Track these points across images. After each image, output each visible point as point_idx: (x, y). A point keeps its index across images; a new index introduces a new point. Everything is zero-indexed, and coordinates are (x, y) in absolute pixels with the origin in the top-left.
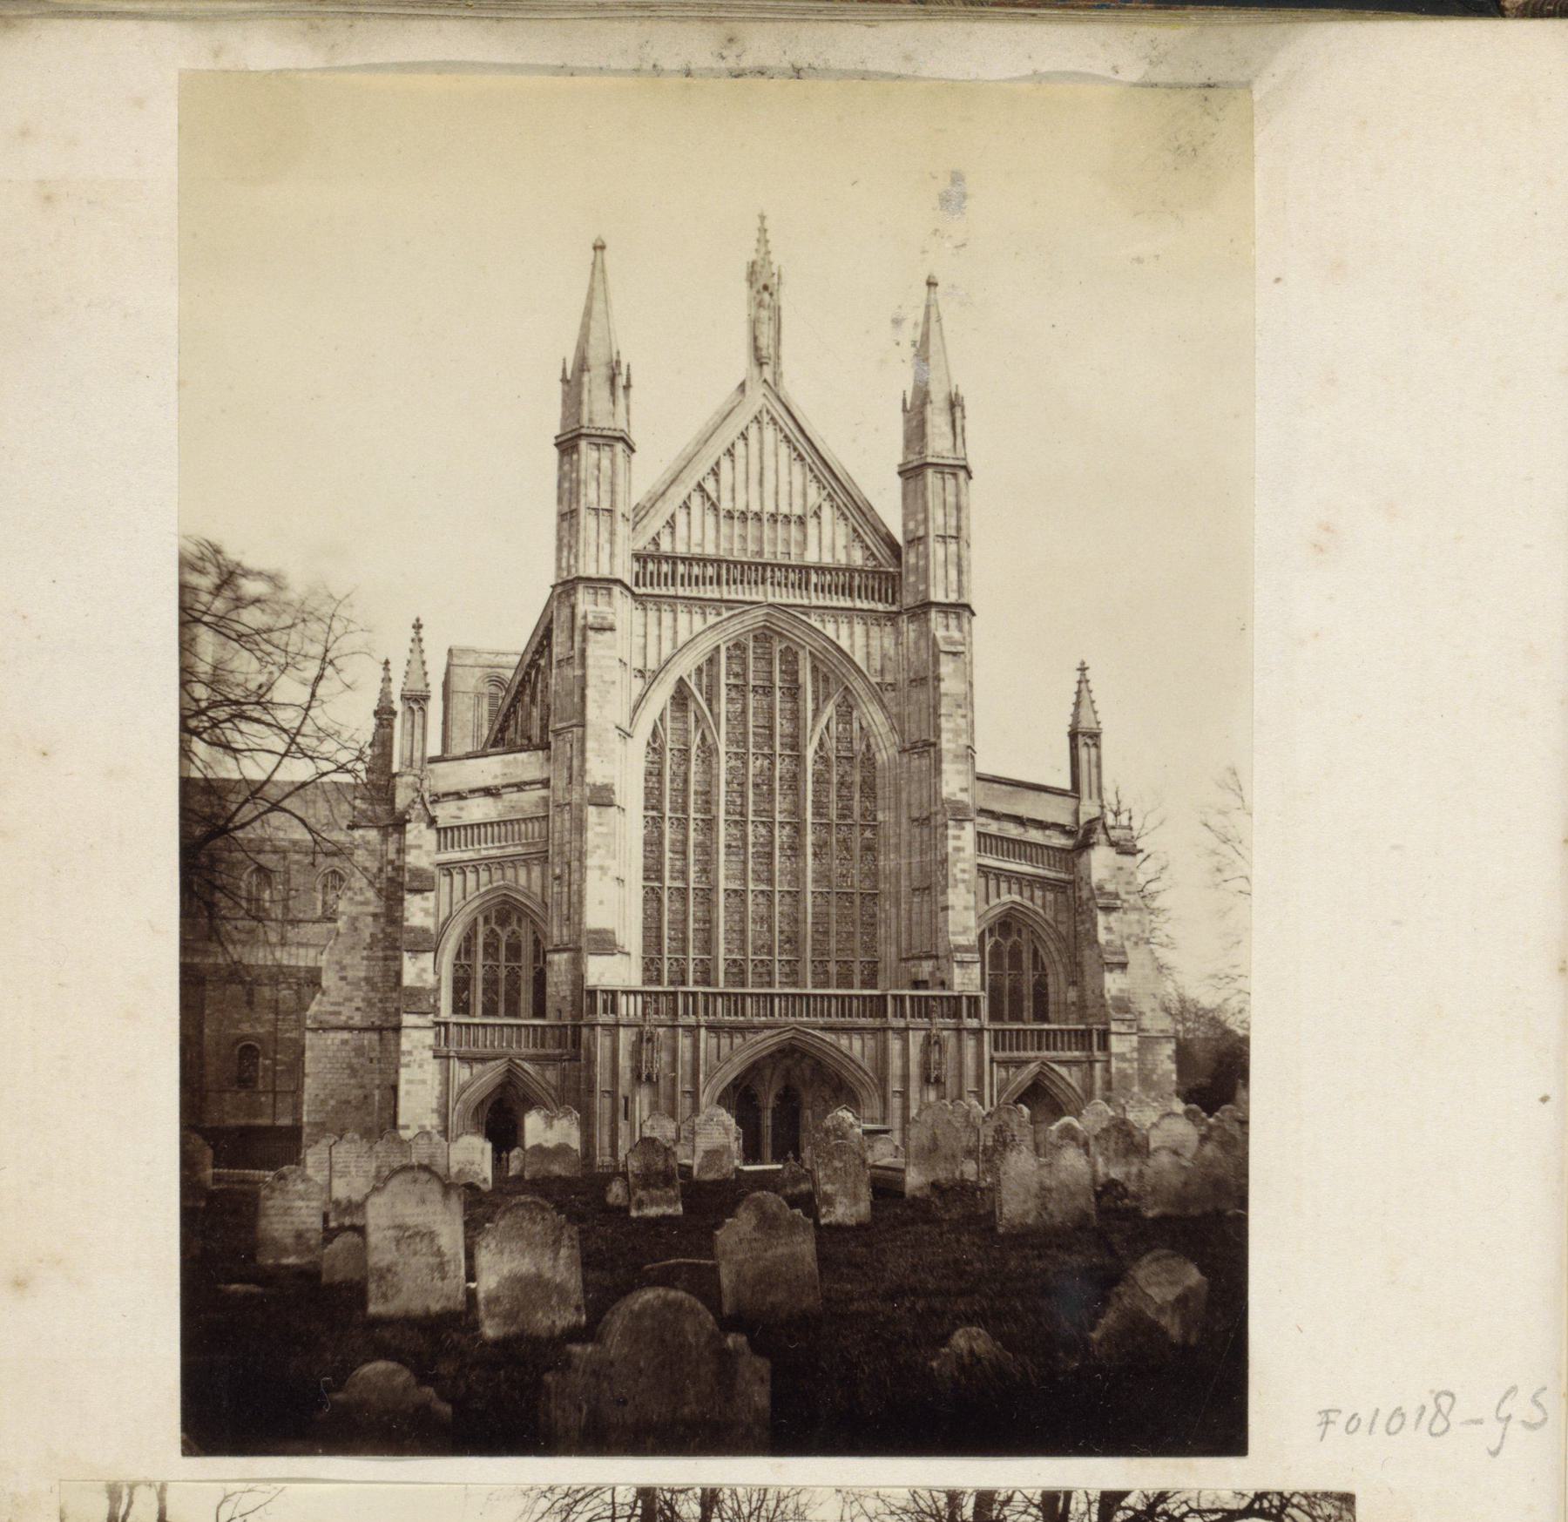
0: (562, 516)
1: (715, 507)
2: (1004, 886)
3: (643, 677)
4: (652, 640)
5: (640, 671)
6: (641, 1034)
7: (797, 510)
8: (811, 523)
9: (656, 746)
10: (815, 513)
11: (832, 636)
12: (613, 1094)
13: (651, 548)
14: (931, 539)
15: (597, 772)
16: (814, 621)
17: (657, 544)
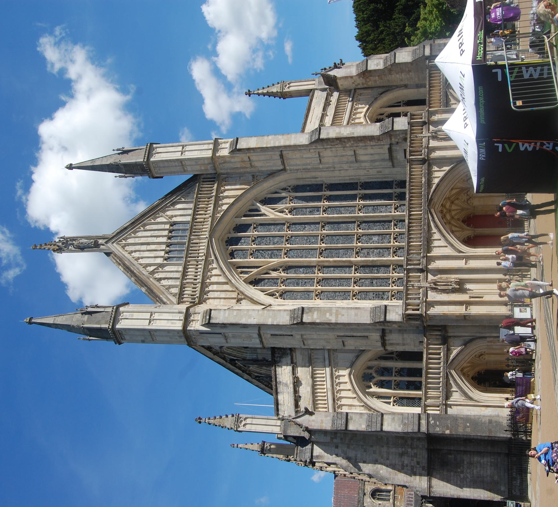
0: (153, 341)
1: (161, 266)
2: (357, 121)
3: (241, 299)
4: (223, 295)
5: (237, 301)
6: (432, 289)
7: (167, 226)
8: (175, 219)
9: (277, 294)
10: (169, 218)
11: (228, 206)
12: (467, 304)
13: (178, 297)
14: (183, 157)
15: (285, 320)
16: (219, 215)
17: (176, 293)
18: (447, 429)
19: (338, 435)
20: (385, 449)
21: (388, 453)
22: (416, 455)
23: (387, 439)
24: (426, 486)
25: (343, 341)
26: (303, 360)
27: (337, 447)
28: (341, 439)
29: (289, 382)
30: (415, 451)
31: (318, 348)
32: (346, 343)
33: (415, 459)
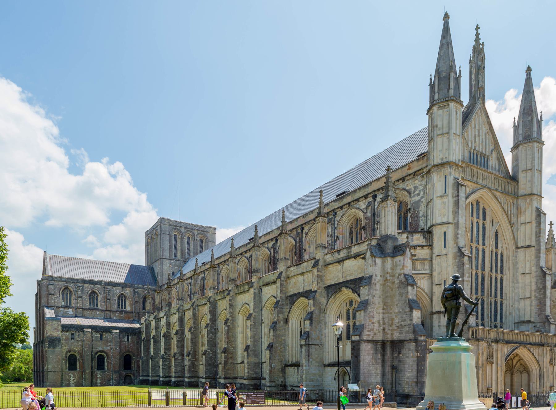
18: (420, 354)
19: (392, 278)
20: (381, 311)
21: (379, 313)
22: (379, 332)
23: (391, 313)
24: (365, 339)
25: (441, 284)
26: (424, 254)
27: (381, 276)
28: (390, 280)
29: (413, 243)
30: (381, 332)
31: (434, 266)
32: (438, 286)
33: (377, 332)
